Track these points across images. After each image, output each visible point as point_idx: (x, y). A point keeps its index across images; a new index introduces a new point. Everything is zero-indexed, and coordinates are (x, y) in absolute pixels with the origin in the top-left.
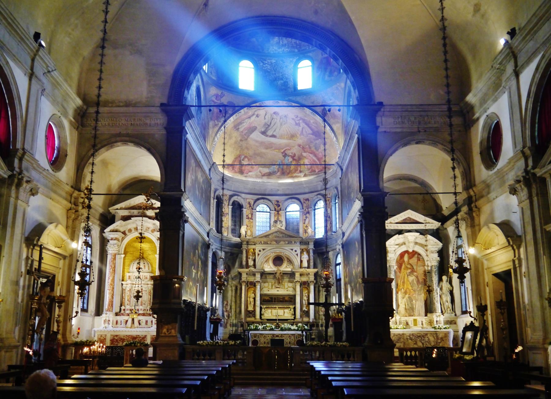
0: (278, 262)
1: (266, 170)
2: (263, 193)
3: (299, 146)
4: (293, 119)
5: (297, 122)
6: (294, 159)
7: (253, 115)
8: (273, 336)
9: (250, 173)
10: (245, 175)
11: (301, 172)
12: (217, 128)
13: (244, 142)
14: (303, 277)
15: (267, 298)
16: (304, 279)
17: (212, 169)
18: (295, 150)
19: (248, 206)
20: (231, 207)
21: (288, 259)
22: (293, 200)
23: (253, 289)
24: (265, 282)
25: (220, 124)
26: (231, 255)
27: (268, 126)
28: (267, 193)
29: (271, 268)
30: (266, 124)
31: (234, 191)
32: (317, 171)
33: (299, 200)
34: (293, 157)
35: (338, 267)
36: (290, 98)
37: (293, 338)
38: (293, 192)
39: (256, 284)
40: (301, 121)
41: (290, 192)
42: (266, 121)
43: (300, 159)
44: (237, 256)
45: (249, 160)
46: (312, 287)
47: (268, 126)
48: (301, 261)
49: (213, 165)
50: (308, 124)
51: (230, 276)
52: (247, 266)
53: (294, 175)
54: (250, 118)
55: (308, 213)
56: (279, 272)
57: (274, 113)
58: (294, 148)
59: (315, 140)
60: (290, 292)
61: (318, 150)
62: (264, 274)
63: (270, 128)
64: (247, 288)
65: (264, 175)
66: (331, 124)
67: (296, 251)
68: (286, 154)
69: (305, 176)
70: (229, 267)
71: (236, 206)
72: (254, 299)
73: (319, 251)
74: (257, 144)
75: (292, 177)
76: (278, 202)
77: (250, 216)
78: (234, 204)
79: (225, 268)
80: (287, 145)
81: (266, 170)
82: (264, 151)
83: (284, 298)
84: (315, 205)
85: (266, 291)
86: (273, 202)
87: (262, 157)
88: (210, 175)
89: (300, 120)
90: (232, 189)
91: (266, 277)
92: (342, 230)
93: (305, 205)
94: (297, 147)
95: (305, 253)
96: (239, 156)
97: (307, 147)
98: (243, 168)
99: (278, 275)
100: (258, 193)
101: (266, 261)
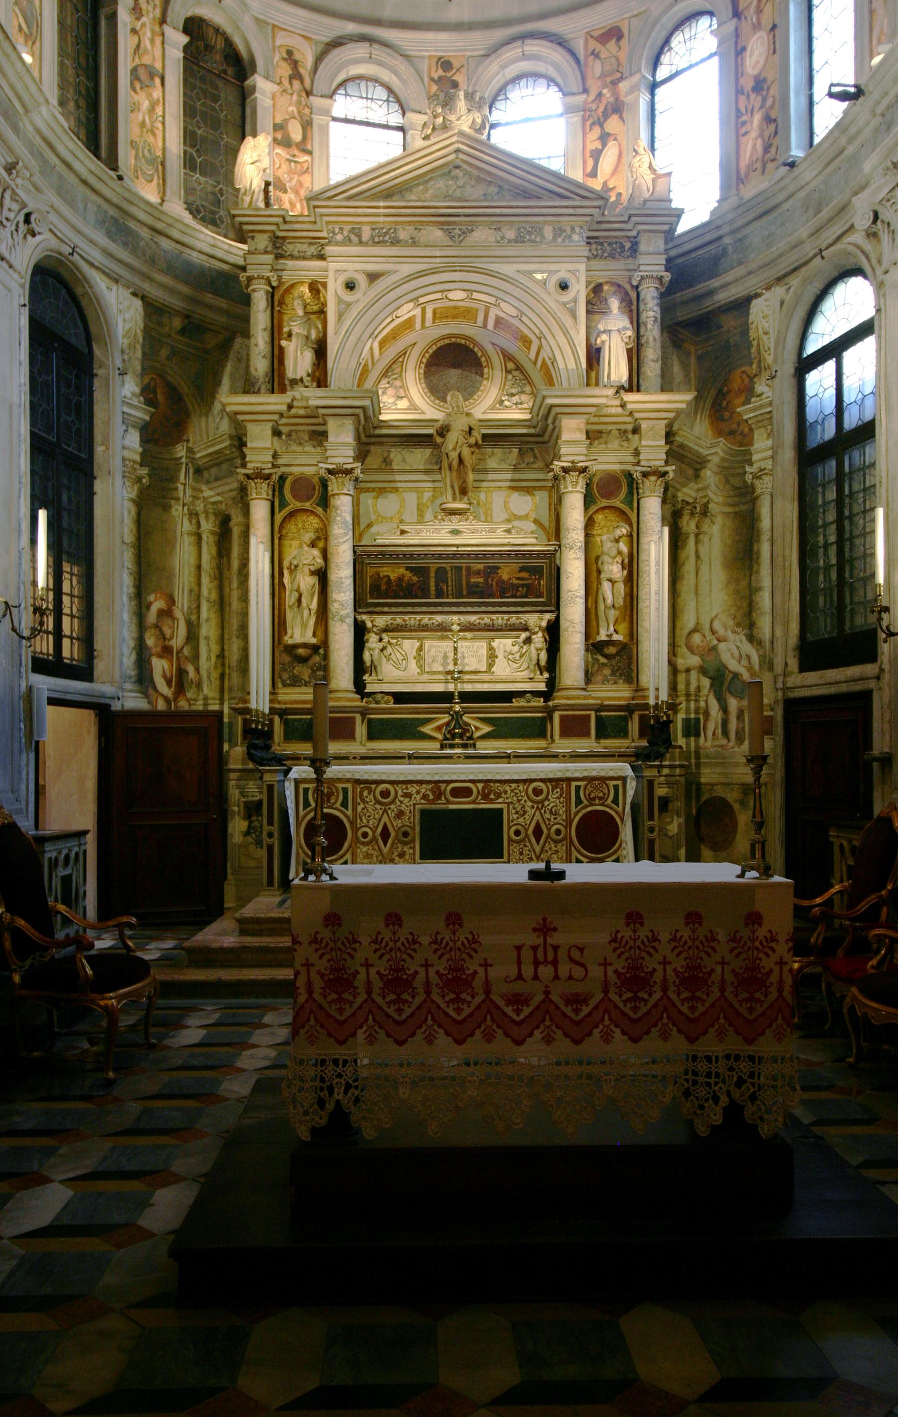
0: (453, 375)
2: (364, 10)
8: (438, 794)
14: (598, 446)
15: (393, 572)
16: (610, 460)
19: (285, 70)
21: (507, 356)
22: (532, 47)
23: (314, 522)
24: (381, 491)
26: (182, 331)
28: (387, 14)
29: (413, 407)
33: (561, 42)
35: (820, 380)
37: (554, 800)
39: (333, 488)
41: (516, 12)
44: (225, 346)
46: (652, 507)
48: (594, 356)
51: (180, 451)
52: (278, 380)
55: (617, 108)
56: (459, 425)
60: (528, 539)
62: (372, 437)
64: (279, 518)
67: (564, 287)
70: (174, 396)
71: (215, 62)
72: (322, 575)
73: (682, 315)
76: (446, 65)
77: (296, 132)
78: (194, 27)
79: (148, 394)
83: (493, 570)
84: (656, 63)
85: (386, 536)
86: (424, 66)
91: (387, 462)
93: (597, 68)
95: (614, 304)
99: (453, 439)
101: (385, 374)
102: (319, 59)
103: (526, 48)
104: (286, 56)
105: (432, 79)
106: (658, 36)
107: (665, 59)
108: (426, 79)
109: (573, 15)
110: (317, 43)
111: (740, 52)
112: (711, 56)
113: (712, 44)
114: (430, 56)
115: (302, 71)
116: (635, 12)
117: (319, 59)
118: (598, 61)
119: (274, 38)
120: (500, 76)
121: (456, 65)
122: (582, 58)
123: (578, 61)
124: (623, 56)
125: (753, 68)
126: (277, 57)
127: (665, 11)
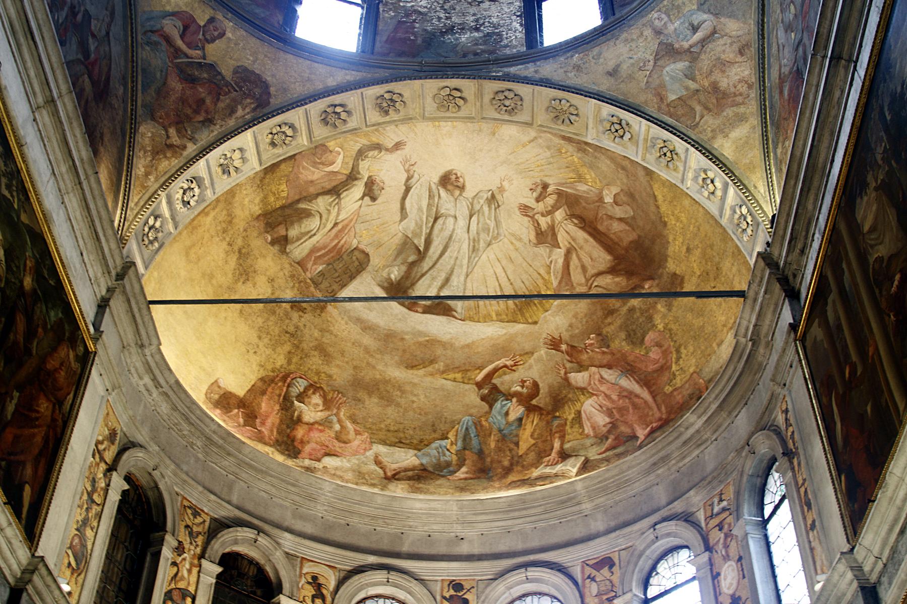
1: (407, 458)
2: (385, 546)
3: (555, 344)
4: (525, 210)
5: (544, 222)
6: (531, 409)
7: (353, 177)
9: (328, 461)
10: (307, 462)
11: (564, 456)
12: (176, 163)
13: (308, 317)
17: (117, 304)
18: (538, 369)
19: (309, 591)
20: (213, 569)
22: (533, 572)
25: (191, 149)
27: (415, 254)
28: (405, 548)
30: (407, 243)
31: (238, 508)
32: (641, 433)
34: (528, 400)
36: (512, 70)
38: (535, 543)
40: (559, 215)
41: (520, 546)
42: (409, 225)
43: (558, 401)
45: (328, 404)
47: (415, 254)
49: (120, 277)
50: (589, 225)
53: (536, 473)
54: (335, 191)
57: (448, 181)
58: (531, 361)
59: (623, 295)
61: (642, 341)
63: (426, 265)
65: (395, 477)
66: (702, 138)
68: (495, 389)
69: (586, 467)
74: (367, 340)
75: (524, 482)
76: (457, 586)
80: (502, 349)
81: (407, 458)
82: (397, 373)
84: (646, 584)
86: (437, 588)
87: (387, 400)
88: (97, 325)
89: (555, 208)
90: (235, 499)
92: (857, 569)
94: (543, 352)
96: (286, 378)
97: (592, 339)
98: (300, 432)
100: (363, 543)
102: (340, 583)
103: (529, 574)
104: (310, 581)
105: (445, 598)
106: (645, 564)
107: (653, 581)
108: (438, 598)
109: (570, 549)
110: (340, 570)
111: (715, 576)
112: (694, 578)
113: (691, 571)
114: (443, 580)
115: (325, 592)
116: (623, 547)
117: (340, 583)
118: (594, 583)
119: (301, 568)
120: (506, 595)
121: (467, 586)
122: (580, 581)
123: (576, 583)
124: (616, 578)
125: (729, 589)
126: (303, 581)
127: (648, 546)
